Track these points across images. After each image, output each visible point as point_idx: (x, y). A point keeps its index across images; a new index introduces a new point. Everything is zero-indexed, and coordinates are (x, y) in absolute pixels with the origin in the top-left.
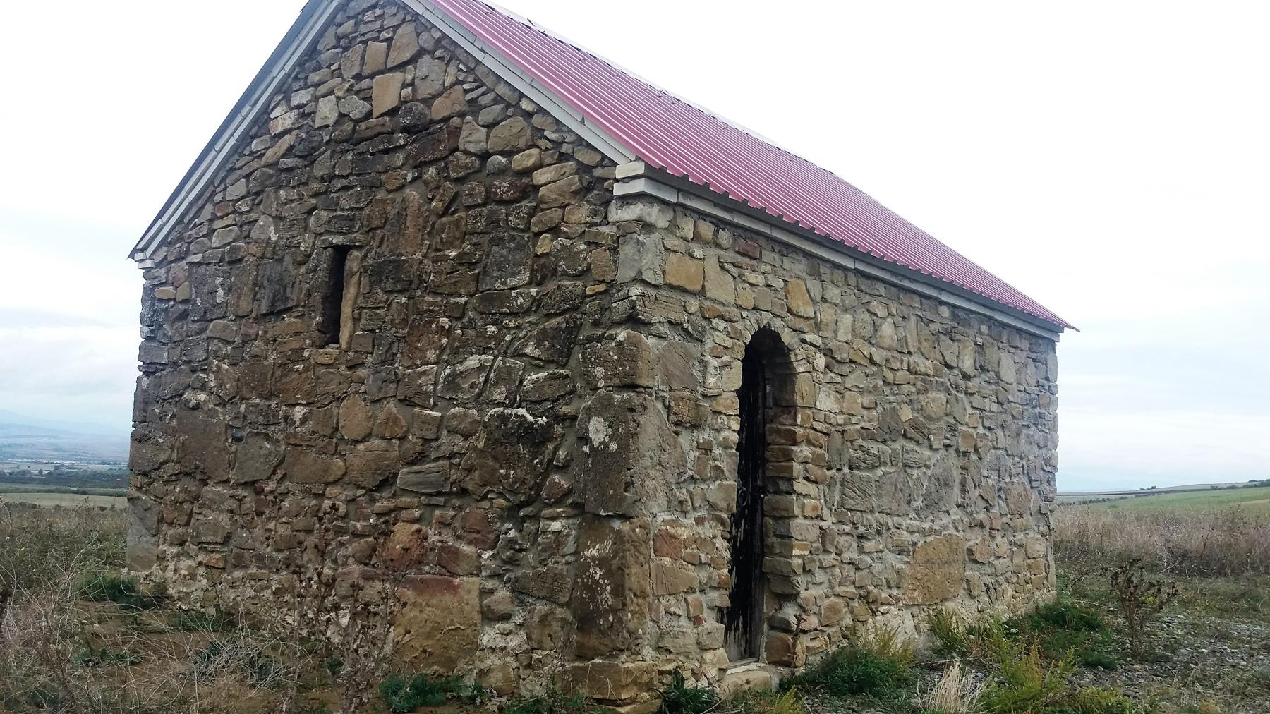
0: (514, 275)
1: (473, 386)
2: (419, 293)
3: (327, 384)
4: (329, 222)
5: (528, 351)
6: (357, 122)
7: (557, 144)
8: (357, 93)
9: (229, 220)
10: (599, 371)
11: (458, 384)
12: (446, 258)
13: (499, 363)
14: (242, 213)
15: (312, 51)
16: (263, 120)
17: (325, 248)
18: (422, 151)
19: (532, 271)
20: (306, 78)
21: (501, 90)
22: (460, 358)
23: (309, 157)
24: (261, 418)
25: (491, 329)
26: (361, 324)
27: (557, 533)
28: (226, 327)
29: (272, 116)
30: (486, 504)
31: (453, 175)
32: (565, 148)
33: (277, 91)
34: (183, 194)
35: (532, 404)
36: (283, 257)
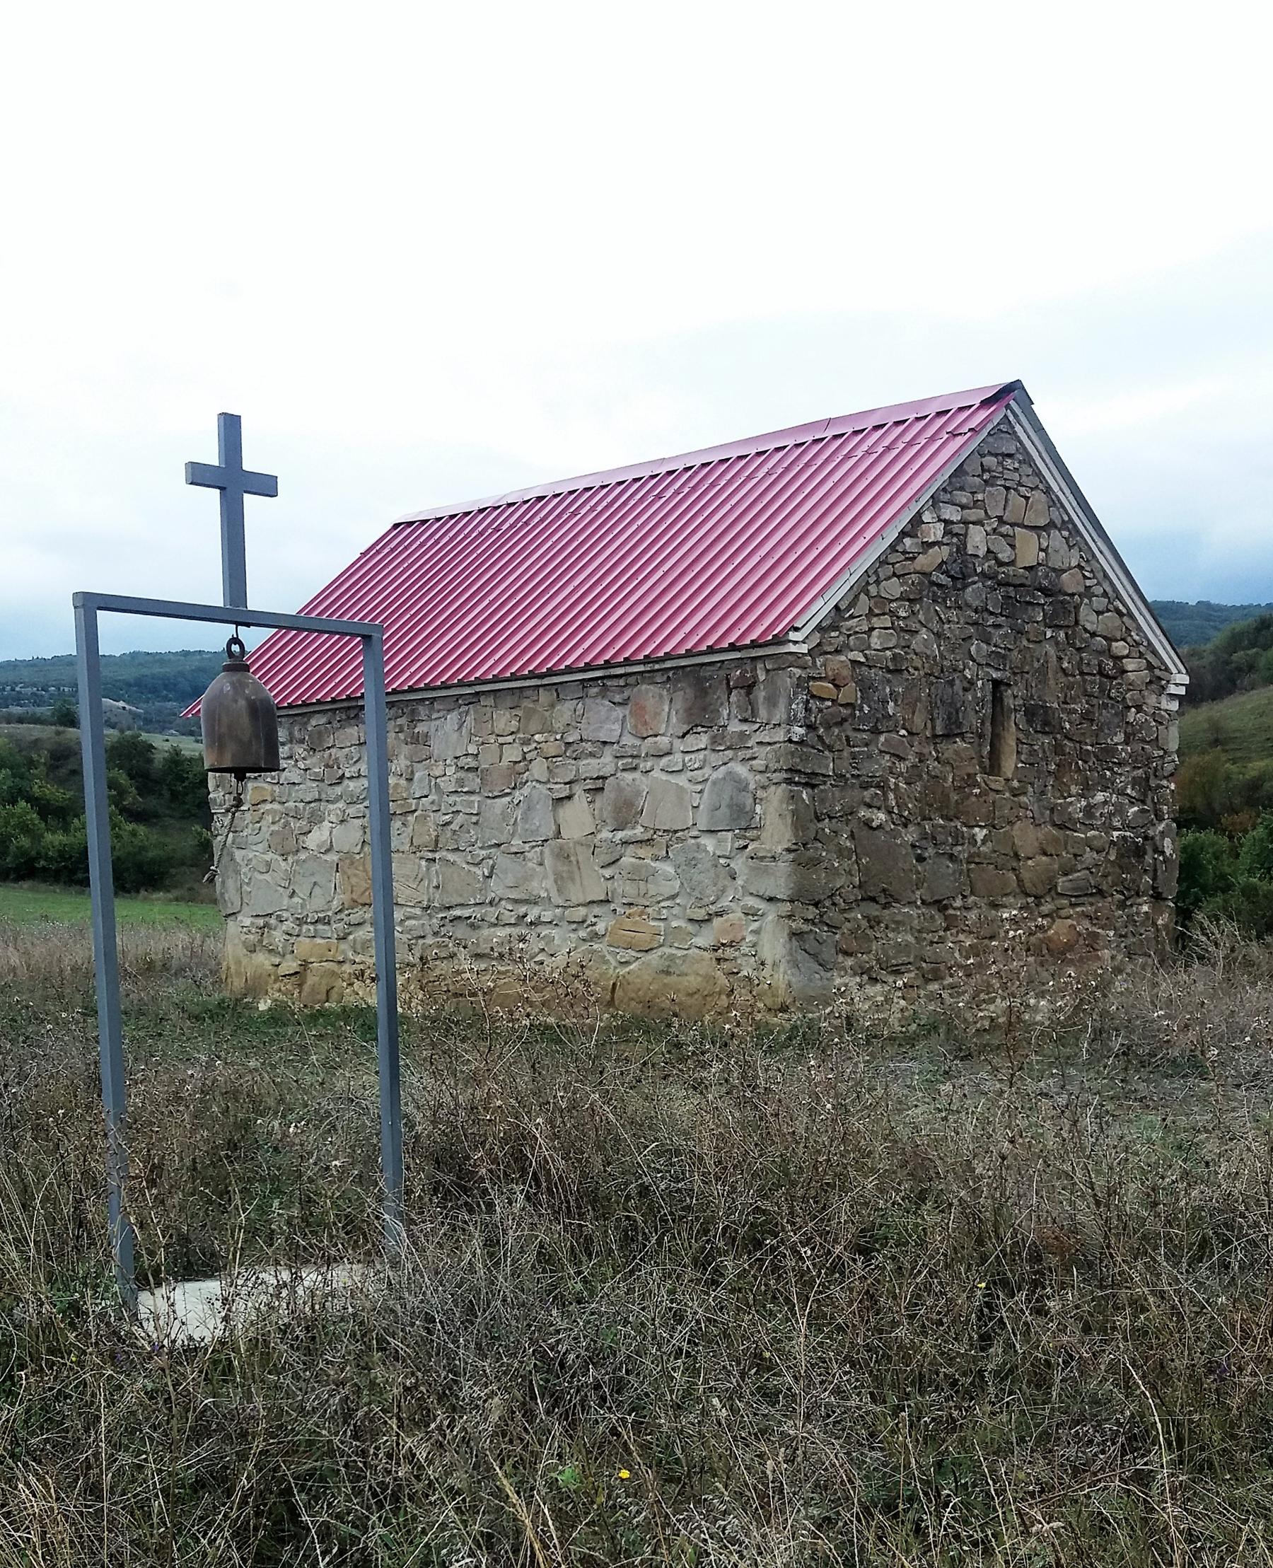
2: (1059, 736)
4: (990, 656)
6: (1001, 564)
7: (1138, 644)
11: (1093, 813)
12: (1075, 711)
14: (898, 617)
15: (960, 471)
17: (988, 681)
18: (1055, 614)
19: (1125, 733)
22: (1092, 793)
23: (960, 579)
24: (950, 839)
25: (1108, 773)
26: (1023, 757)
30: (1110, 899)
31: (1078, 644)
32: (1142, 649)
36: (953, 679)
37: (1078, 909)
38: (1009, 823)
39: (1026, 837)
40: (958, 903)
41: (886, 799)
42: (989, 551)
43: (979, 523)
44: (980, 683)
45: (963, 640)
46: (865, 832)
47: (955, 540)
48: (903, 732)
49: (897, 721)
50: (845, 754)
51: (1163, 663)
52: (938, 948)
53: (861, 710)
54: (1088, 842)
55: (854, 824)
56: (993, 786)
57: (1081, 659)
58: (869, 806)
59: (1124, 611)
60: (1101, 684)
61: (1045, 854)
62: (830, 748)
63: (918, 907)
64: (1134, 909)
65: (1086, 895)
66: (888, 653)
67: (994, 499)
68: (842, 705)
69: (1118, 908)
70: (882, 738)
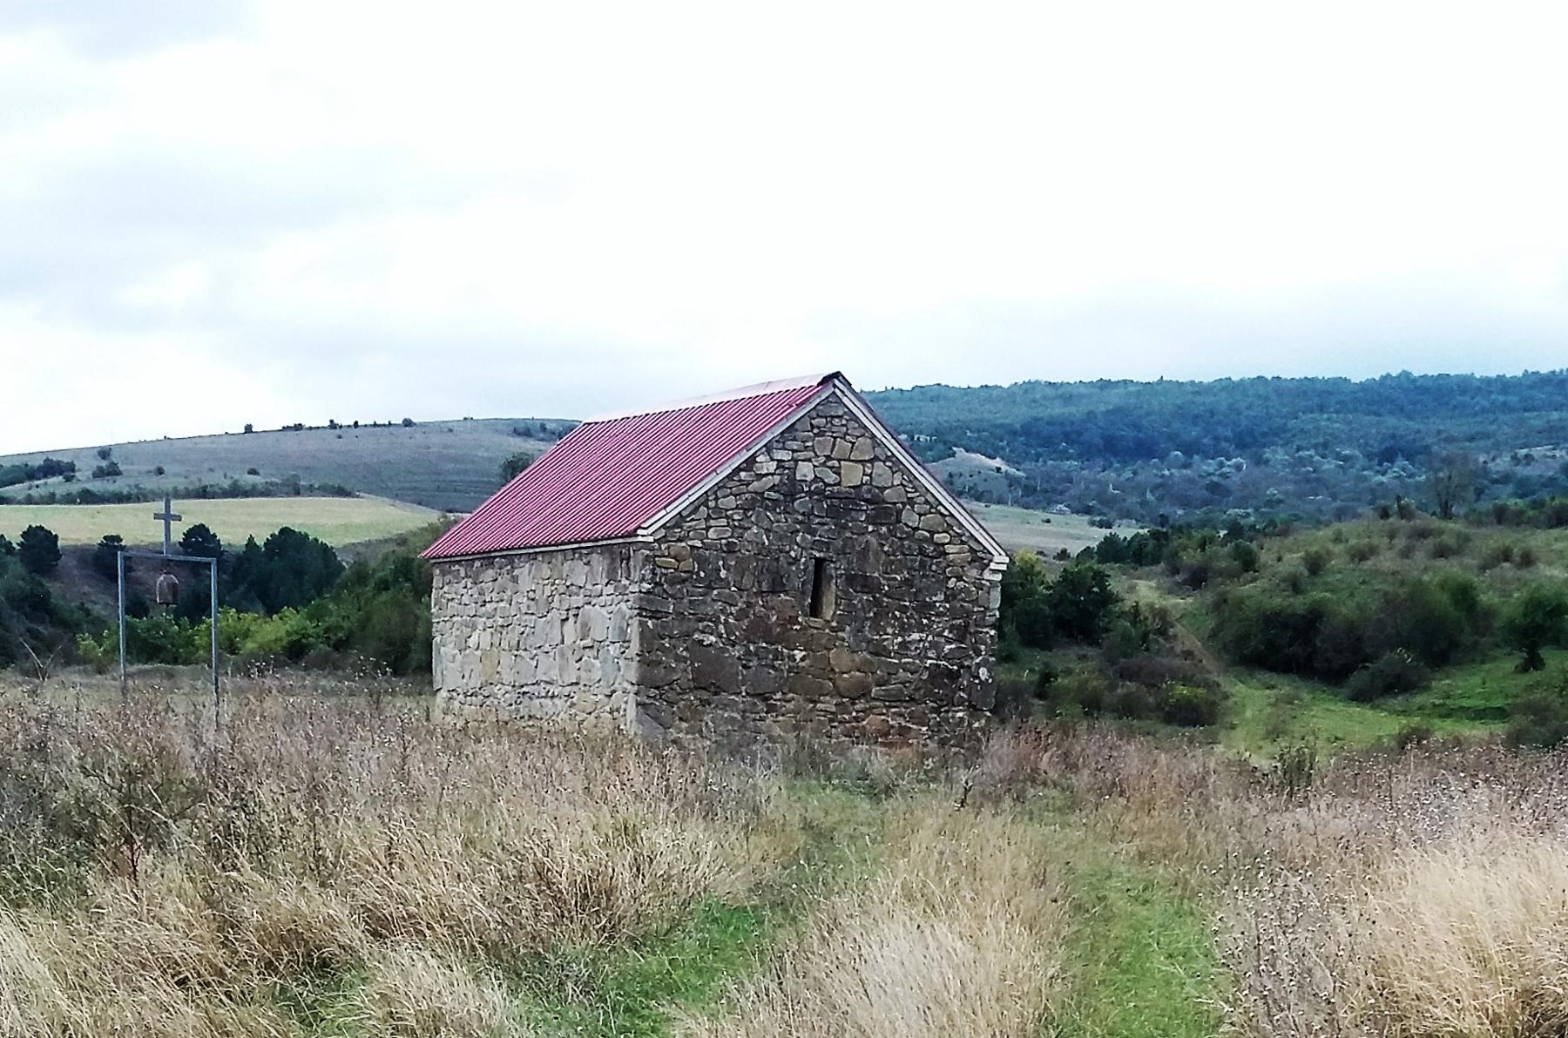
0: (935, 596)
1: (916, 648)
3: (820, 639)
5: (946, 634)
6: (827, 485)
7: (960, 535)
8: (829, 467)
9: (724, 522)
10: (983, 647)
12: (896, 579)
13: (930, 638)
14: (734, 520)
16: (751, 461)
18: (877, 516)
20: (784, 443)
21: (931, 499)
24: (771, 656)
25: (925, 621)
27: (961, 718)
28: (731, 596)
29: (758, 459)
33: (765, 446)
34: (686, 496)
35: (948, 660)
37: (893, 710)
38: (826, 648)
39: (839, 658)
40: (779, 696)
41: (717, 628)
42: (816, 476)
43: (810, 460)
44: (803, 560)
45: (792, 533)
46: (698, 648)
47: (787, 471)
48: (733, 589)
49: (729, 583)
50: (685, 601)
51: (985, 548)
52: (759, 724)
53: (698, 574)
54: (900, 665)
55: (689, 642)
56: (812, 625)
57: (903, 545)
58: (703, 632)
59: (947, 513)
60: (921, 562)
61: (859, 671)
62: (672, 596)
63: (743, 697)
64: (950, 714)
65: (899, 701)
66: (723, 541)
67: (823, 446)
68: (685, 572)
69: (931, 713)
70: (715, 592)
